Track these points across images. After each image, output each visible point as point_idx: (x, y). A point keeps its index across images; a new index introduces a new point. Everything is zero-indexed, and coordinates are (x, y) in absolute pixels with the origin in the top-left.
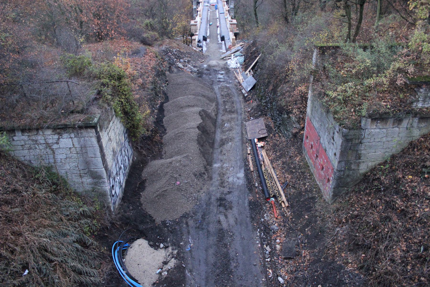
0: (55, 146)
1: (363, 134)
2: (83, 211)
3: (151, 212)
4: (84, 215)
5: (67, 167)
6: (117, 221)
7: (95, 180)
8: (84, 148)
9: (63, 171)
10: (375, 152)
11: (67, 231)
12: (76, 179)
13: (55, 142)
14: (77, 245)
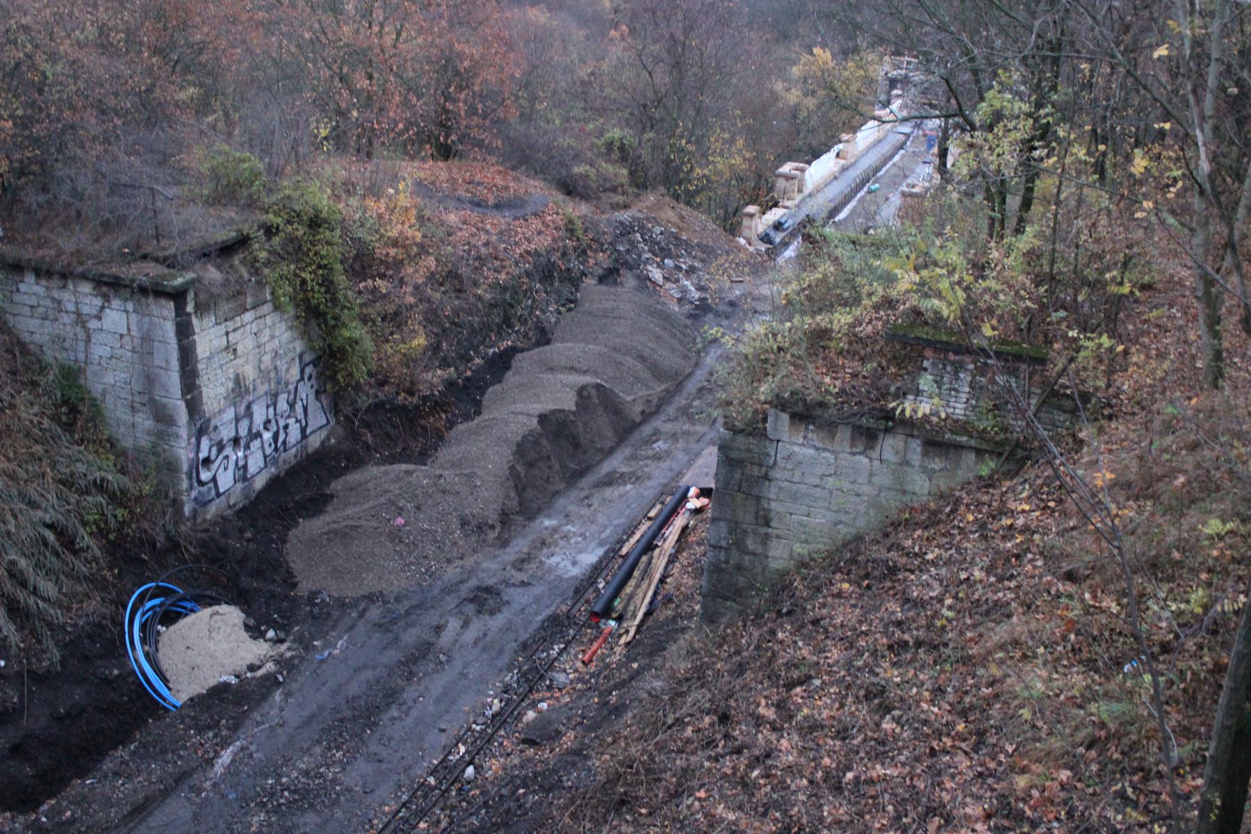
0: (93, 324)
1: (772, 453)
2: (102, 480)
3: (296, 563)
4: (101, 486)
5: (109, 379)
6: (191, 543)
7: (161, 427)
8: (147, 339)
9: (99, 388)
10: (808, 515)
11: (38, 498)
12: (123, 413)
13: (95, 312)
14: (51, 536)
